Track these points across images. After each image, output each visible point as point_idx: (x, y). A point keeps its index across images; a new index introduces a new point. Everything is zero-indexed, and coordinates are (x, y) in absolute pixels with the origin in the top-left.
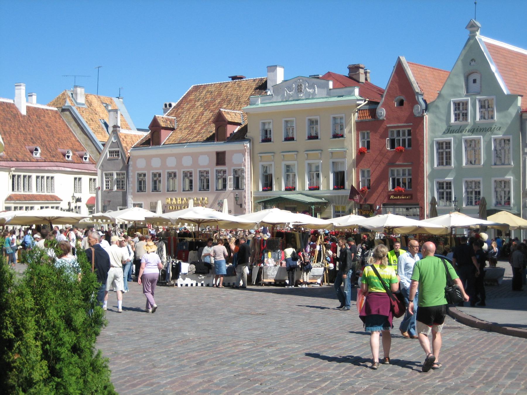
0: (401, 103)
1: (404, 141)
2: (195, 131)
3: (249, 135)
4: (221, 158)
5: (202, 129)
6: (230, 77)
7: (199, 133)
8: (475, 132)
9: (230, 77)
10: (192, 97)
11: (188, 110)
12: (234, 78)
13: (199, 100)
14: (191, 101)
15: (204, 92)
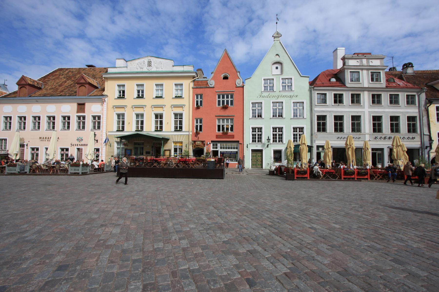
0: (226, 78)
1: (227, 101)
2: (59, 90)
3: (105, 93)
4: (81, 107)
5: (64, 89)
6: (87, 66)
7: (62, 91)
8: (279, 98)
9: (87, 66)
10: (57, 73)
11: (54, 79)
12: (89, 66)
13: (63, 75)
14: (56, 75)
15: (67, 72)
